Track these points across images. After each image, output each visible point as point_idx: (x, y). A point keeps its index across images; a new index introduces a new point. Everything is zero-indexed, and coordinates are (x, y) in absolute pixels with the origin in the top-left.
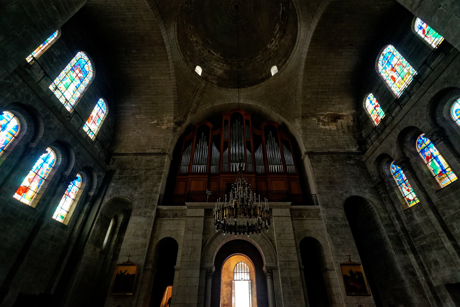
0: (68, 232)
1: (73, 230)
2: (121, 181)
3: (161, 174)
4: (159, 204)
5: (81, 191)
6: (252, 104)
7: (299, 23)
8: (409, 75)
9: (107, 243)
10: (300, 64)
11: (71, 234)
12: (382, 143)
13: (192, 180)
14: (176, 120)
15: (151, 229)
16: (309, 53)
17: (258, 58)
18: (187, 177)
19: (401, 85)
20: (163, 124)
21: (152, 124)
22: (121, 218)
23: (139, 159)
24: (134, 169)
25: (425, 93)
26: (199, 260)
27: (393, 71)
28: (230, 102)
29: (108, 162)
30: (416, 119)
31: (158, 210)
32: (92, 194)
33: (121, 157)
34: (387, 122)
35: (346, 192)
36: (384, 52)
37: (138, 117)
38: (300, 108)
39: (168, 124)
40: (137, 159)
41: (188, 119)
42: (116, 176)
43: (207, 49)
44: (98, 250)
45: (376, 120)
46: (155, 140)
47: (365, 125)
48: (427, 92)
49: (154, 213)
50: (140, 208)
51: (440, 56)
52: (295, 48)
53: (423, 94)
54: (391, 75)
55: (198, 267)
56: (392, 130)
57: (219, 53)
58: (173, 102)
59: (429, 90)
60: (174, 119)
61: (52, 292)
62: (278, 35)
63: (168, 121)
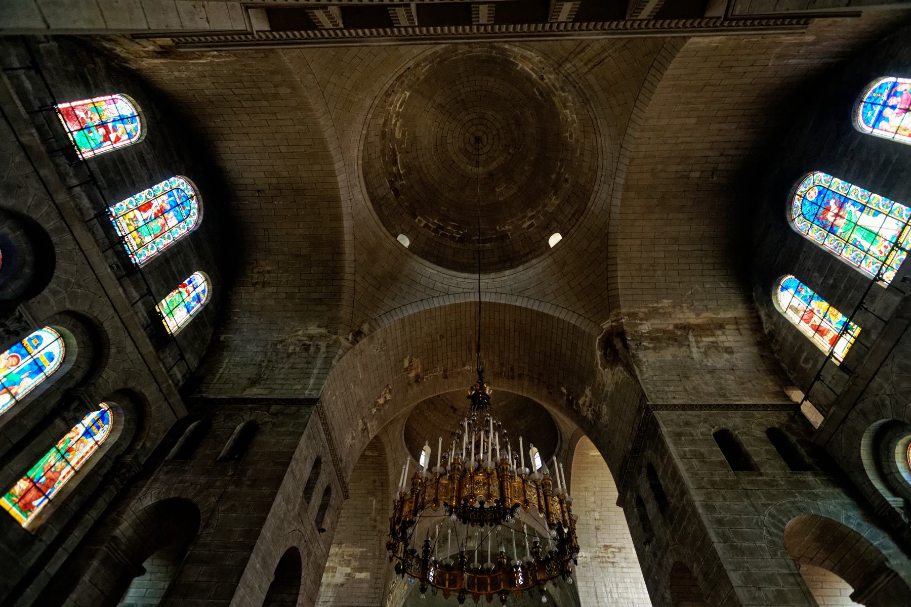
7: (371, 207)
8: (137, 245)
10: (340, 146)
12: (23, 154)
16: (332, 174)
19: (128, 222)
25: (115, 310)
27: (158, 210)
30: (68, 283)
34: (62, 160)
36: (194, 204)
38: (292, 67)
43: (546, 84)
45: (70, 114)
47: (71, 68)
48: (116, 315)
51: (145, 315)
52: (360, 162)
53: (113, 306)
54: (155, 203)
56: (57, 207)
57: (518, 68)
59: (117, 319)
62: (393, 123)
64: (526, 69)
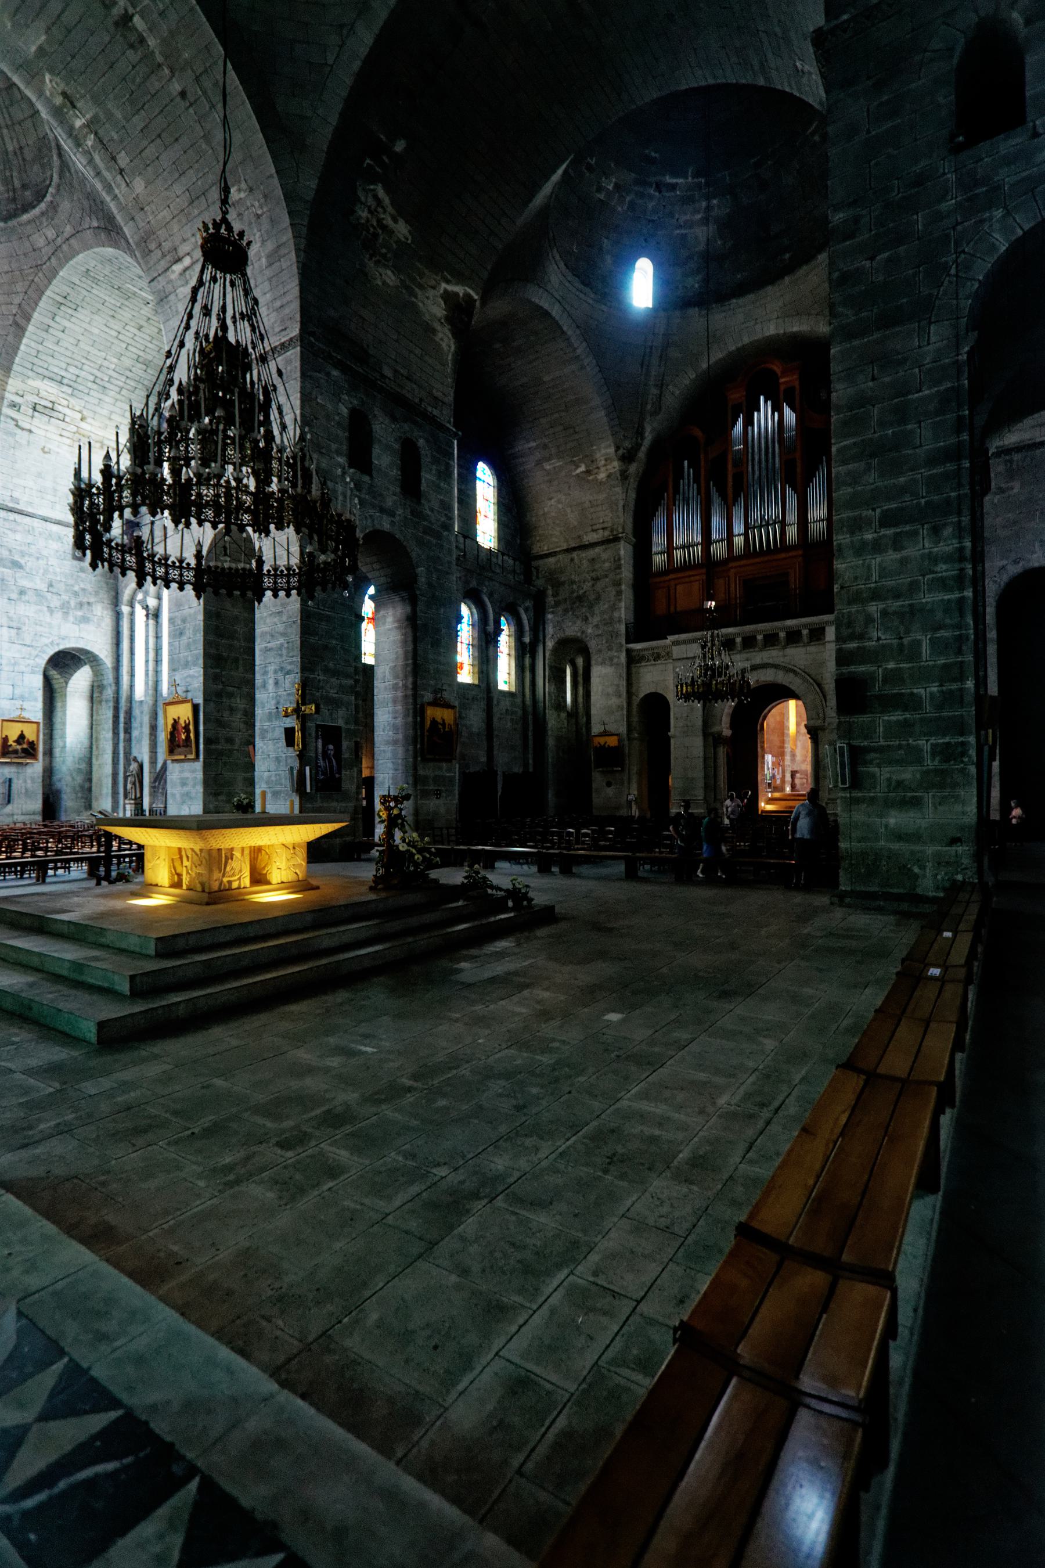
0: (519, 700)
1: (524, 695)
2: (560, 609)
3: (620, 584)
4: (627, 642)
5: (512, 640)
6: (801, 329)
9: (572, 701)
11: (524, 702)
13: (676, 585)
14: (621, 452)
15: (625, 683)
17: (813, 134)
18: (667, 578)
20: (598, 468)
21: (577, 475)
22: (580, 661)
23: (576, 561)
24: (573, 582)
26: (700, 723)
28: (740, 345)
29: (528, 580)
31: (629, 652)
32: (527, 640)
33: (546, 560)
35: (1016, 562)
37: (548, 467)
39: (609, 467)
40: (572, 560)
41: (647, 434)
42: (550, 600)
43: (651, 187)
44: (563, 715)
46: (592, 510)
49: (623, 658)
50: (600, 651)
55: (700, 733)
58: (603, 413)
60: (616, 451)
61: (531, 770)
63: (606, 460)
64: (680, 181)
